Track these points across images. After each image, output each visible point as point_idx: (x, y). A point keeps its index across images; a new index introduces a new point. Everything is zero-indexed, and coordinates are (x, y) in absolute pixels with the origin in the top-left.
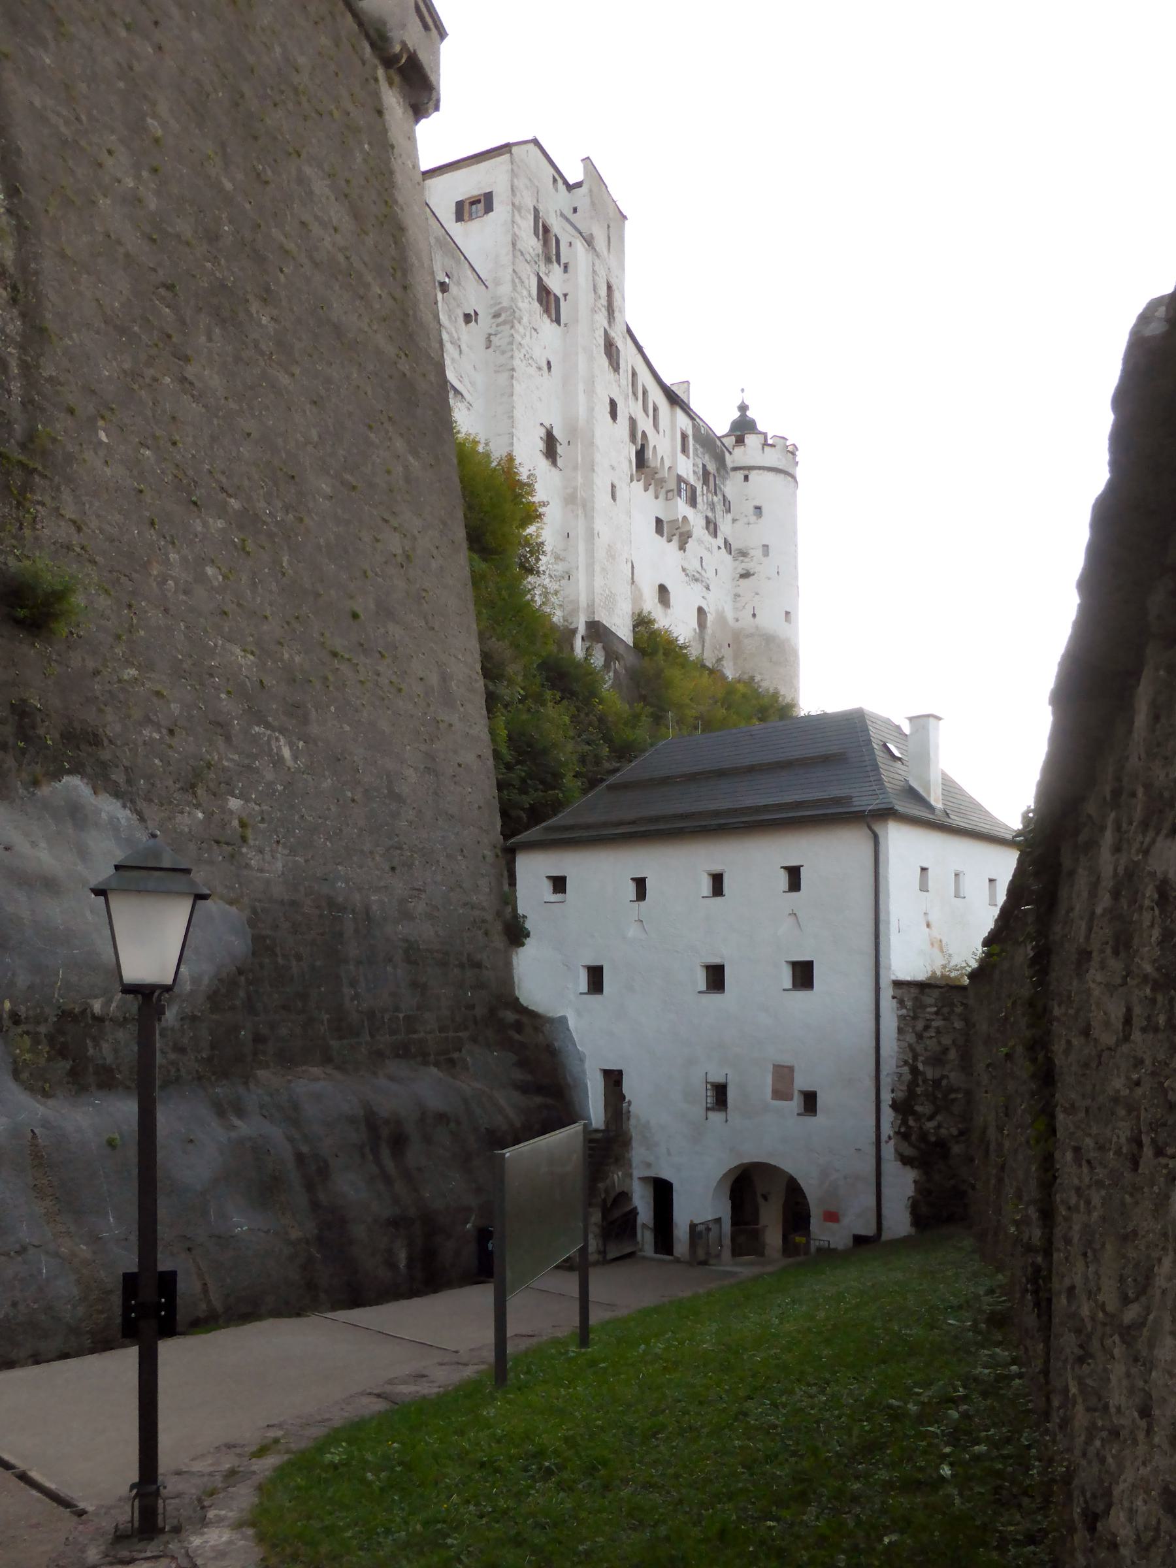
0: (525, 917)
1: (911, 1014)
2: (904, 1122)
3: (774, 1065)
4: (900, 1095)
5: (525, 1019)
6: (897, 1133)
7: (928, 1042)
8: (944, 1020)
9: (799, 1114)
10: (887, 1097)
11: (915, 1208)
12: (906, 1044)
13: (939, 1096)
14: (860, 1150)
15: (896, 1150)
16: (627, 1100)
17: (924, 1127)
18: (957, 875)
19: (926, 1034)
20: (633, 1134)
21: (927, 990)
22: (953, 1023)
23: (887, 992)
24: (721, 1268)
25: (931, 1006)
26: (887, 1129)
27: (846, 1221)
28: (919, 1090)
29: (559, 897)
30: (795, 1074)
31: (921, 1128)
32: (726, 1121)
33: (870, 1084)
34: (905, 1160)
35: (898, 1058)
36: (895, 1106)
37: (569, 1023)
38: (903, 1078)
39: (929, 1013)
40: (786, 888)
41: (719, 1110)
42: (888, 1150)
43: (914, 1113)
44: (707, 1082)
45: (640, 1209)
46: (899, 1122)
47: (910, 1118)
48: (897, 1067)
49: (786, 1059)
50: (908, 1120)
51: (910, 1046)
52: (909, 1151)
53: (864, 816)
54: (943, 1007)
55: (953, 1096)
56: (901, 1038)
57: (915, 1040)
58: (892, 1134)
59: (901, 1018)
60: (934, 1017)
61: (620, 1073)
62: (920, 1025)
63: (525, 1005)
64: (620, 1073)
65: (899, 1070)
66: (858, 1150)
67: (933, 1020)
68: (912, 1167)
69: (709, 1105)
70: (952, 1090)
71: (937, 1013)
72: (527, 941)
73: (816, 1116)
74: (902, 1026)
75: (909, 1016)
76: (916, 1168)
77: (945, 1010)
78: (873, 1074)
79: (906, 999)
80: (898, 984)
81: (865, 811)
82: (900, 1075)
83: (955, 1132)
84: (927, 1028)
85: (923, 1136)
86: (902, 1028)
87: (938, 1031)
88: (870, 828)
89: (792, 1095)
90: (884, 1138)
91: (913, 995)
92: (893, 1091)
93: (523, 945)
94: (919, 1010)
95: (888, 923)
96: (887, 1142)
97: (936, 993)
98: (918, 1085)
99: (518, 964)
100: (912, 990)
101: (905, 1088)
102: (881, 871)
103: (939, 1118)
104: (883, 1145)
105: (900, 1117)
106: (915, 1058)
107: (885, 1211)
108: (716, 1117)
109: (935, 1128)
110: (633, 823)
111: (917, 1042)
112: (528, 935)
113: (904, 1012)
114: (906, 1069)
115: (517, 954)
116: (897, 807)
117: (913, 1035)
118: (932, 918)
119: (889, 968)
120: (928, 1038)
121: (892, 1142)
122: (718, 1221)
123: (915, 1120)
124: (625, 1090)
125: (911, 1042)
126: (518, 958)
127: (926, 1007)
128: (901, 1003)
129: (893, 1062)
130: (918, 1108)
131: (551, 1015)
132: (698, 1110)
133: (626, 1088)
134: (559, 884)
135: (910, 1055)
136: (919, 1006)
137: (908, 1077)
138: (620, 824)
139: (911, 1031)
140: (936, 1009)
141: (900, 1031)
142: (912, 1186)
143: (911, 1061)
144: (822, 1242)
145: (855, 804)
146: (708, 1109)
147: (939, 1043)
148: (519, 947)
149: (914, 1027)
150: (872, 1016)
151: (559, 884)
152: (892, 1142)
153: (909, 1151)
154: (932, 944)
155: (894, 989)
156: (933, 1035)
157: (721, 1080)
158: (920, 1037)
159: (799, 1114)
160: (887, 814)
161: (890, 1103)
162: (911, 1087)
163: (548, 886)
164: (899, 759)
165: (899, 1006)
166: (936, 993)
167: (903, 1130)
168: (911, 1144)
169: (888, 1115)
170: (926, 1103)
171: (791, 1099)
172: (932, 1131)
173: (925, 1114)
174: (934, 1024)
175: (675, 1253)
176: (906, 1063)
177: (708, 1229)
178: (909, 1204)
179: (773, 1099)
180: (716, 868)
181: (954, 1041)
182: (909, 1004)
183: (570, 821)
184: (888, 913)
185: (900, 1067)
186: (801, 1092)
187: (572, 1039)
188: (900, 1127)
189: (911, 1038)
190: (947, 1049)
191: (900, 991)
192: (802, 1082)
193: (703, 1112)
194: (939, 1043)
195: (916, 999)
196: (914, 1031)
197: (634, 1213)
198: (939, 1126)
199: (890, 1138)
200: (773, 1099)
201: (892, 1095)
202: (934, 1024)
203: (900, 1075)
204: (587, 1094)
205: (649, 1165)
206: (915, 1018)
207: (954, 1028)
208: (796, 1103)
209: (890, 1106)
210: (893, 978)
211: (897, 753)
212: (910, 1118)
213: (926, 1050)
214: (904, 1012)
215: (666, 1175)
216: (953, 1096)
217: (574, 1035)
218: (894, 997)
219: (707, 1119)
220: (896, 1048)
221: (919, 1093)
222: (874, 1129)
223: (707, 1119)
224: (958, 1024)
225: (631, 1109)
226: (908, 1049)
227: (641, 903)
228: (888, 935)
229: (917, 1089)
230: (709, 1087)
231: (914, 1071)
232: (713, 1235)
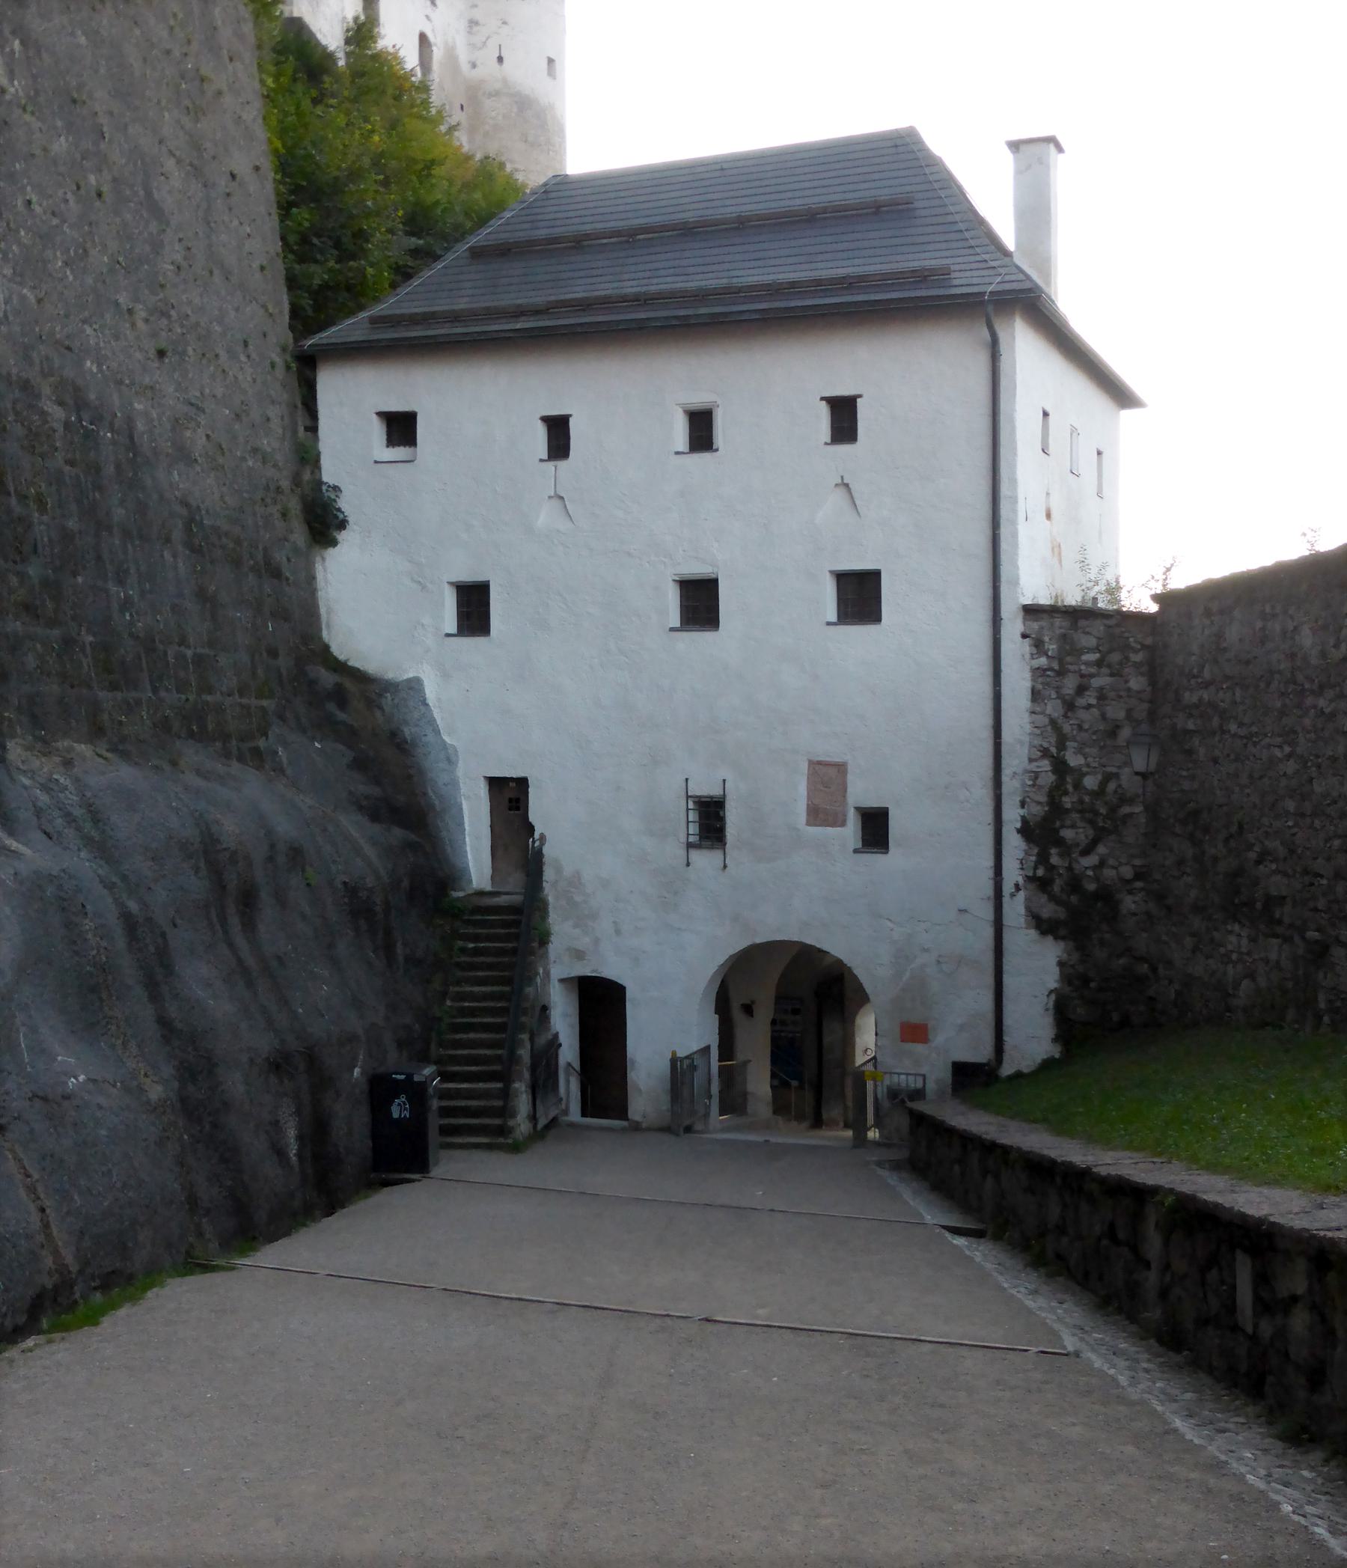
0: (336, 489)
1: (1056, 667)
2: (1043, 859)
3: (811, 763)
4: (1037, 811)
5: (348, 684)
6: (1029, 879)
7: (1083, 715)
8: (1112, 675)
9: (856, 851)
10: (1013, 815)
11: (1061, 1010)
12: (1046, 721)
13: (1103, 811)
14: (965, 911)
15: (1028, 909)
16: (537, 835)
17: (1075, 866)
19: (1081, 702)
20: (551, 899)
21: (1082, 623)
22: (1127, 682)
23: (1013, 627)
24: (708, 1136)
25: (1090, 650)
26: (1012, 874)
27: (939, 1039)
28: (1067, 802)
30: (850, 777)
31: (1070, 869)
32: (725, 867)
33: (982, 794)
34: (1044, 926)
35: (1032, 746)
36: (1026, 831)
37: (427, 691)
38: (1040, 781)
39: (1087, 664)
41: (711, 848)
42: (1015, 909)
43: (1060, 842)
44: (688, 797)
45: (563, 1039)
46: (1033, 858)
47: (1053, 851)
48: (1031, 760)
49: (830, 751)
50: (1050, 854)
51: (1053, 722)
52: (1048, 910)
53: (982, 303)
54: (1111, 651)
55: (1126, 810)
56: (1038, 709)
57: (1062, 711)
58: (1021, 880)
59: (1038, 672)
60: (1093, 670)
61: (522, 783)
62: (1070, 684)
63: (342, 657)
64: (522, 783)
65: (1033, 767)
66: (962, 911)
67: (1092, 676)
68: (1056, 938)
69: (692, 838)
70: (1124, 800)
71: (1099, 663)
72: (342, 536)
73: (887, 853)
74: (1040, 687)
75: (1051, 669)
76: (1063, 938)
77: (1115, 658)
78: (989, 773)
79: (1046, 639)
80: (1031, 611)
81: (983, 294)
82: (1036, 776)
83: (1127, 872)
84: (1081, 690)
85: (1075, 884)
86: (1039, 691)
87: (1102, 697)
89: (845, 815)
90: (1008, 888)
91: (1058, 632)
92: (1023, 804)
93: (333, 543)
94: (1069, 659)
96: (1012, 895)
97: (1098, 627)
98: (1066, 793)
99: (326, 581)
100: (1058, 622)
101: (1043, 799)
103: (1101, 849)
104: (1006, 899)
105: (1036, 851)
106: (1061, 745)
107: (1008, 1021)
108: (705, 860)
109: (1094, 868)
111: (1065, 716)
112: (342, 525)
113: (1043, 661)
114: (1045, 765)
115: (323, 559)
117: (1059, 701)
119: (1015, 582)
120: (1084, 708)
121: (1021, 895)
122: (706, 1050)
123: (1061, 855)
124: (533, 817)
125: (1055, 715)
126: (325, 571)
127: (1081, 652)
128: (1038, 645)
129: (1024, 752)
130: (1067, 834)
131: (390, 675)
132: (673, 850)
133: (536, 813)
135: (1053, 740)
136: (1069, 649)
137: (1048, 779)
139: (1054, 696)
140: (1098, 655)
141: (1036, 695)
142: (1055, 971)
143: (1054, 750)
144: (895, 1078)
146: (690, 846)
147: (1103, 716)
148: (326, 548)
149: (1058, 689)
150: (987, 670)
152: (1021, 895)
153: (1048, 910)
155: (1025, 620)
156: (1093, 701)
157: (715, 791)
158: (1070, 706)
159: (856, 851)
161: (1019, 825)
162: (1055, 795)
165: (1035, 651)
166: (1098, 627)
167: (1040, 872)
168: (1053, 898)
169: (1014, 845)
170: (1079, 824)
171: (843, 824)
172: (1090, 873)
173: (1078, 845)
174: (1096, 682)
175: (630, 1115)
176: (1045, 753)
177: (693, 1068)
178: (1051, 1005)
179: (808, 824)
181: (1129, 712)
182: (1052, 648)
185: (1035, 760)
186: (857, 809)
187: (432, 722)
188: (1035, 868)
189: (1054, 708)
190: (1118, 727)
191: (1035, 626)
192: (861, 792)
193: (681, 852)
194: (1103, 716)
195: (1064, 638)
196: (1060, 696)
197: (554, 1044)
198: (1102, 864)
199: (1017, 887)
200: (808, 824)
201: (1022, 812)
202: (1096, 682)
203: (1036, 776)
204: (461, 824)
205: (579, 955)
206: (1061, 673)
207: (1129, 690)
208: (851, 831)
209: (1019, 831)
210: (1027, 601)
212: (1053, 851)
213: (1080, 727)
214: (1043, 661)
215: (612, 970)
216: (1126, 810)
217: (437, 714)
218: (1024, 636)
219: (688, 864)
220: (1028, 728)
221: (1068, 806)
222: (991, 873)
223: (688, 864)
224: (1137, 683)
225: (546, 850)
226: (1049, 728)
227: (562, 464)
228: (1014, 523)
229: (1065, 799)
230: (691, 805)
231: (1060, 767)
232: (699, 1078)
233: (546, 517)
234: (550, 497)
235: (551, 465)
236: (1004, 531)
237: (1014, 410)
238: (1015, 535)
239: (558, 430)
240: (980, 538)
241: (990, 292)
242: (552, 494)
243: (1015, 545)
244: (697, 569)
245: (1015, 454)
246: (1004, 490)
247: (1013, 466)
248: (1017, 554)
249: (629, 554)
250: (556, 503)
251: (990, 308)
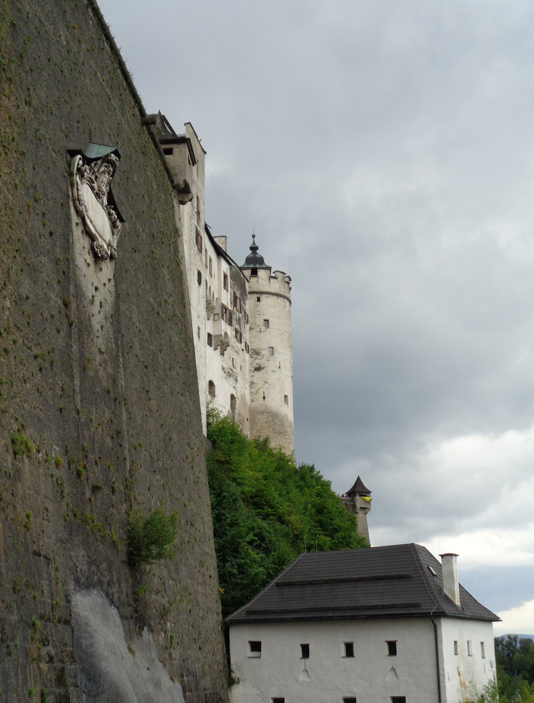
18: (468, 642)
29: (255, 654)
40: (388, 654)
88: (433, 622)
95: (444, 675)
102: (439, 646)
110: (301, 611)
116: (446, 611)
118: (461, 670)
134: (256, 646)
138: (294, 611)
145: (423, 607)
151: (256, 646)
154: (461, 685)
160: (441, 615)
163: (248, 647)
164: (436, 576)
180: (349, 640)
183: (260, 607)
184: (443, 669)
211: (434, 573)
227: (307, 660)
228: (444, 682)
233: (302, 677)
234: (303, 670)
235: (303, 660)
236: (441, 684)
237: (442, 646)
238: (445, 686)
239: (306, 651)
240: (433, 686)
241: (433, 613)
242: (304, 669)
243: (445, 689)
244: (349, 695)
245: (443, 661)
246: (441, 672)
247: (443, 664)
248: (445, 692)
249: (328, 690)
250: (305, 673)
251: (432, 618)
